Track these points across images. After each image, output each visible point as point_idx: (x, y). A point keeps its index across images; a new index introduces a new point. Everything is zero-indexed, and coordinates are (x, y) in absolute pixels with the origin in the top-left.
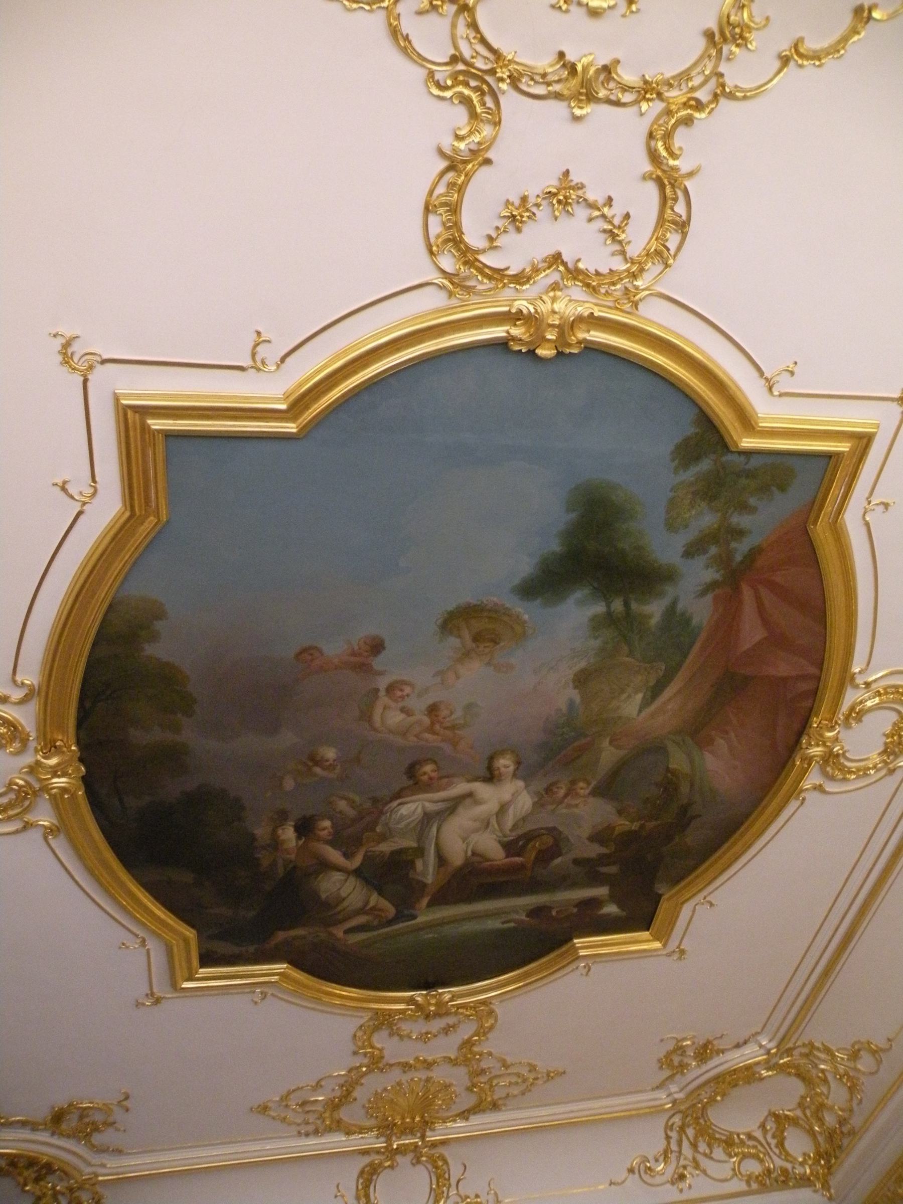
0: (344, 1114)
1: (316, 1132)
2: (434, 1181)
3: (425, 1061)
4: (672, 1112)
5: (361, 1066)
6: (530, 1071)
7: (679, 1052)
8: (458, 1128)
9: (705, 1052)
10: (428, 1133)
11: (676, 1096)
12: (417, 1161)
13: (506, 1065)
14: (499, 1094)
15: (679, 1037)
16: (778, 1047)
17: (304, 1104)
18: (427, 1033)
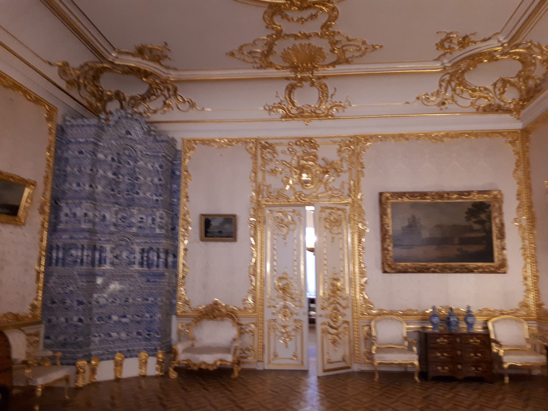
0: (271, 59)
1: (261, 67)
2: (321, 94)
3: (305, 34)
4: (443, 74)
5: (273, 34)
6: (363, 44)
7: (449, 41)
8: (330, 71)
9: (465, 42)
10: (315, 72)
11: (447, 65)
12: (312, 84)
13: (349, 40)
14: (348, 55)
15: (448, 32)
16: (509, 43)
17: (250, 53)
18: (302, 18)
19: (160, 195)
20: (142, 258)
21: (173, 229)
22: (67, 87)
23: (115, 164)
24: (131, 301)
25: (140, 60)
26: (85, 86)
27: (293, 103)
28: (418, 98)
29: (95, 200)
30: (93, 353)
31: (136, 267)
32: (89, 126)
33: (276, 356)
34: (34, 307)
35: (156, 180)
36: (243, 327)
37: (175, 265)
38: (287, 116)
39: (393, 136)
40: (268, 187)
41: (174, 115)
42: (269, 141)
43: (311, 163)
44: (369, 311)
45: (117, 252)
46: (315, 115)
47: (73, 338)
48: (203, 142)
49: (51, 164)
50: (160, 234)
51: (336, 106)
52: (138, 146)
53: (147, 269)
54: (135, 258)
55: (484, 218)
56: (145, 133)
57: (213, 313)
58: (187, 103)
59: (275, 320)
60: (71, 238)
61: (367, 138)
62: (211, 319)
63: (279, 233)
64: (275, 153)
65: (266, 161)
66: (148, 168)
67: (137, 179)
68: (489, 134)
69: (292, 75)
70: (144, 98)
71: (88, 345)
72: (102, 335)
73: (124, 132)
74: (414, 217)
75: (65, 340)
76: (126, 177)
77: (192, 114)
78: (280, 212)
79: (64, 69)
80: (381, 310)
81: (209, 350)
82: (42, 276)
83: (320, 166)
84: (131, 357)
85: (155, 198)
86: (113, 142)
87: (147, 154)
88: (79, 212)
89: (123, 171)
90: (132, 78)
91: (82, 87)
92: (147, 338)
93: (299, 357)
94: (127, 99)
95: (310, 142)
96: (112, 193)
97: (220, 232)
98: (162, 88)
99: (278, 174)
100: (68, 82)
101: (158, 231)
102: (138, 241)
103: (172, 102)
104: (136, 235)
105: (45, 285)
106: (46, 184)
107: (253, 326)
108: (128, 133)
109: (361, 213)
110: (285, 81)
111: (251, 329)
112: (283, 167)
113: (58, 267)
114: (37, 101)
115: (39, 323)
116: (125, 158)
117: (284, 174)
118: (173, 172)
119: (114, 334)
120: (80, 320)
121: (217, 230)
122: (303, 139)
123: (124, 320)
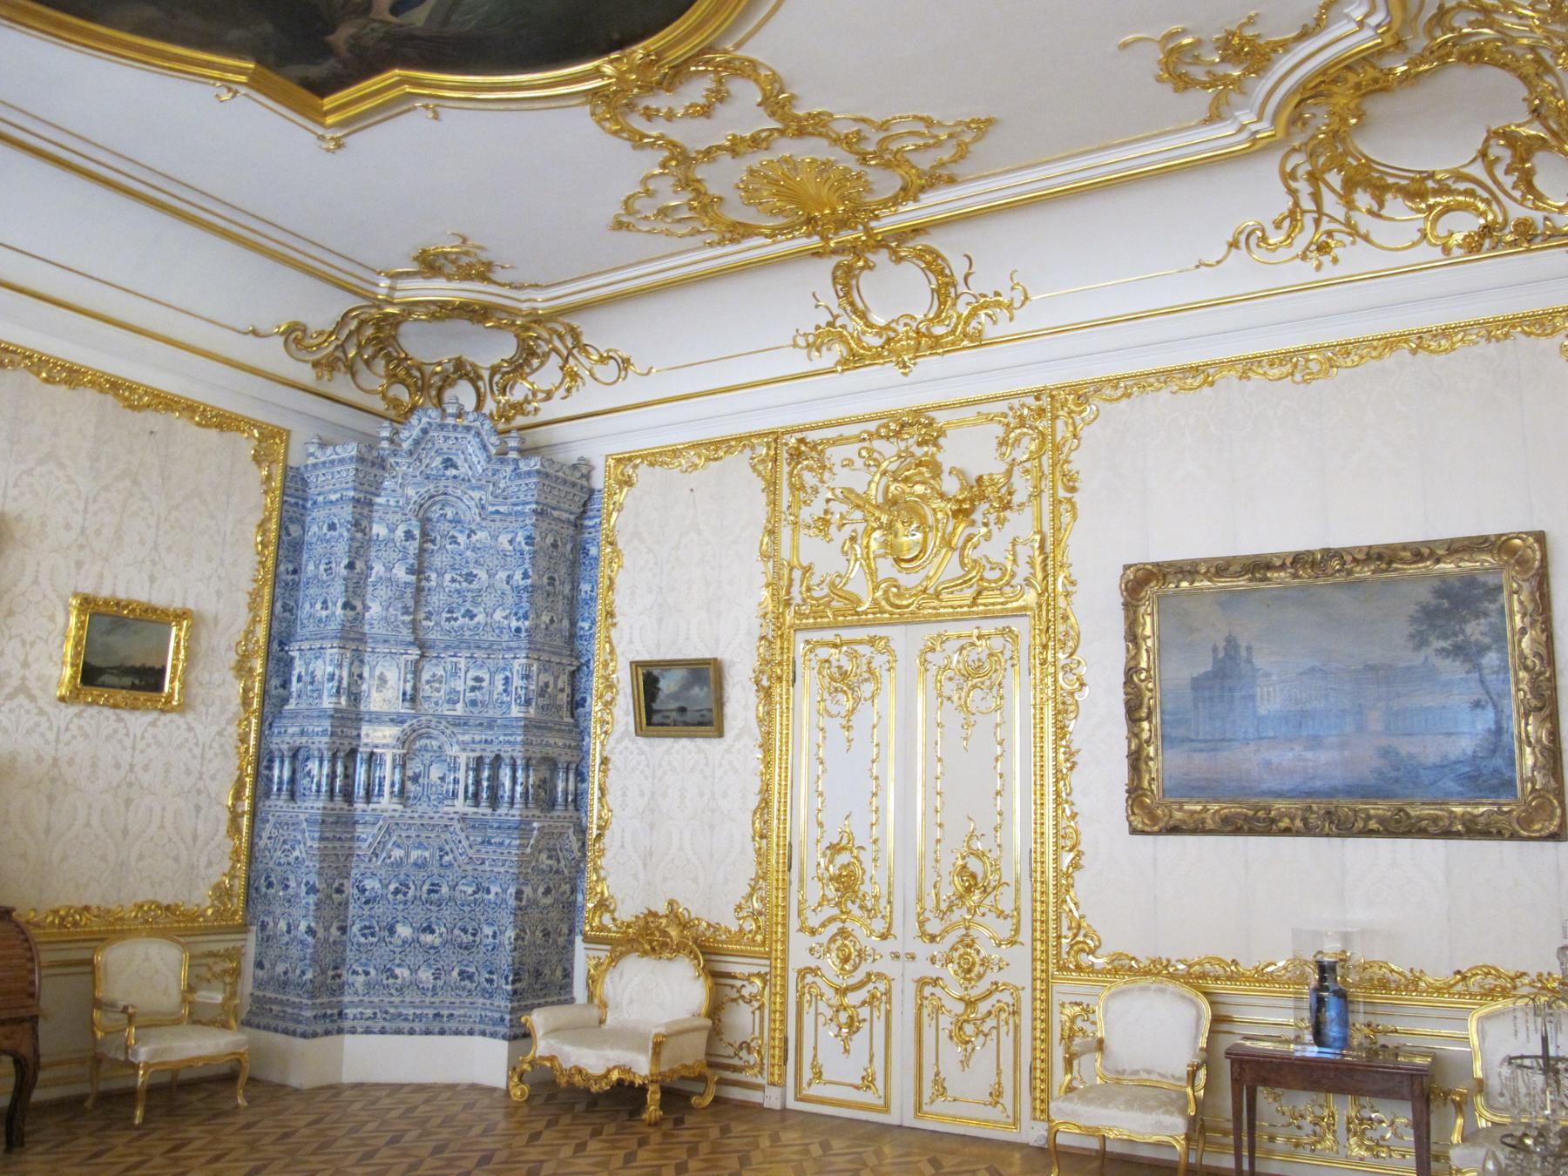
19: (526, 617)
20: (477, 782)
21: (577, 704)
22: (319, 378)
23: (413, 547)
24: (445, 890)
25: (440, 283)
26: (367, 363)
27: (863, 316)
28: (1234, 244)
29: (362, 639)
30: (350, 1012)
31: (460, 805)
32: (342, 461)
33: (819, 1075)
34: (222, 893)
35: (518, 576)
36: (739, 983)
37: (578, 801)
38: (854, 360)
39: (1166, 375)
40: (807, 570)
41: (589, 396)
42: (812, 436)
43: (919, 489)
44: (1083, 955)
45: (414, 767)
46: (927, 342)
47: (298, 972)
48: (654, 458)
49: (270, 563)
50: (517, 719)
51: (985, 306)
52: (476, 495)
53: (489, 811)
54: (456, 781)
55: (1476, 637)
56: (489, 459)
57: (651, 937)
58: (612, 362)
59: (814, 971)
60: (302, 733)
61: (1081, 394)
62: (645, 953)
63: (833, 709)
64: (824, 467)
65: (802, 495)
66: (493, 550)
67: (470, 577)
68: (1498, 329)
69: (815, 242)
70: (519, 366)
71: (341, 989)
72: (373, 972)
73: (438, 461)
74: (1231, 642)
75: (285, 973)
76: (448, 577)
77: (631, 390)
78: (835, 646)
79: (295, 336)
80: (1119, 956)
81: (624, 1037)
82: (245, 821)
83: (942, 496)
84: (442, 1032)
85: (514, 624)
86: (411, 492)
87: (498, 512)
88: (322, 668)
89: (438, 561)
90: (465, 325)
91: (361, 366)
92: (484, 990)
93: (880, 1083)
94: (486, 374)
95: (918, 426)
96: (408, 618)
97: (682, 710)
98: (545, 335)
99: (833, 529)
100: (316, 364)
101: (516, 711)
102: (467, 738)
103: (580, 364)
104: (460, 723)
105: (252, 845)
106: (253, 606)
107: (758, 982)
108: (449, 463)
109: (1071, 642)
110: (816, 260)
111: (755, 990)
112: (844, 508)
113: (280, 803)
114: (223, 422)
115: (243, 928)
116: (444, 526)
117: (848, 530)
118: (580, 549)
119: (402, 972)
120: (310, 931)
121: (674, 705)
122: (892, 416)
123: (428, 938)
